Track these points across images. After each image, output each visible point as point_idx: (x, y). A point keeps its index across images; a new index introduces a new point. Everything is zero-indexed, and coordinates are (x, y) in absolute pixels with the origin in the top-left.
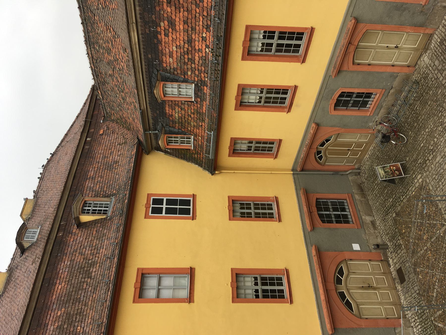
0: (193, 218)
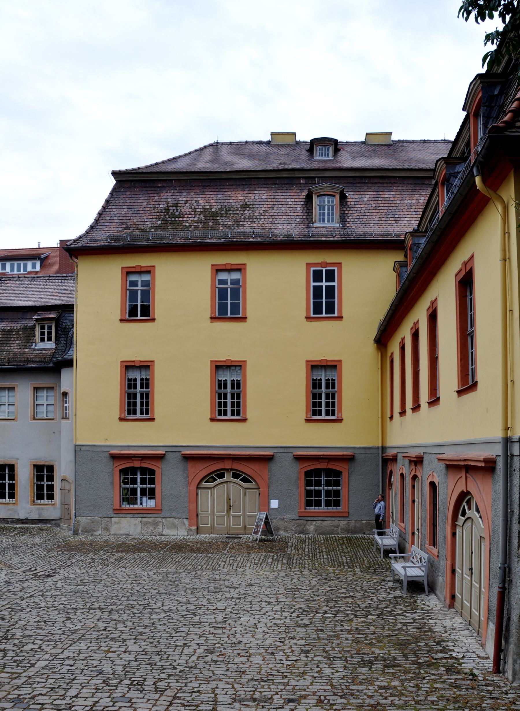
0: (308, 318)
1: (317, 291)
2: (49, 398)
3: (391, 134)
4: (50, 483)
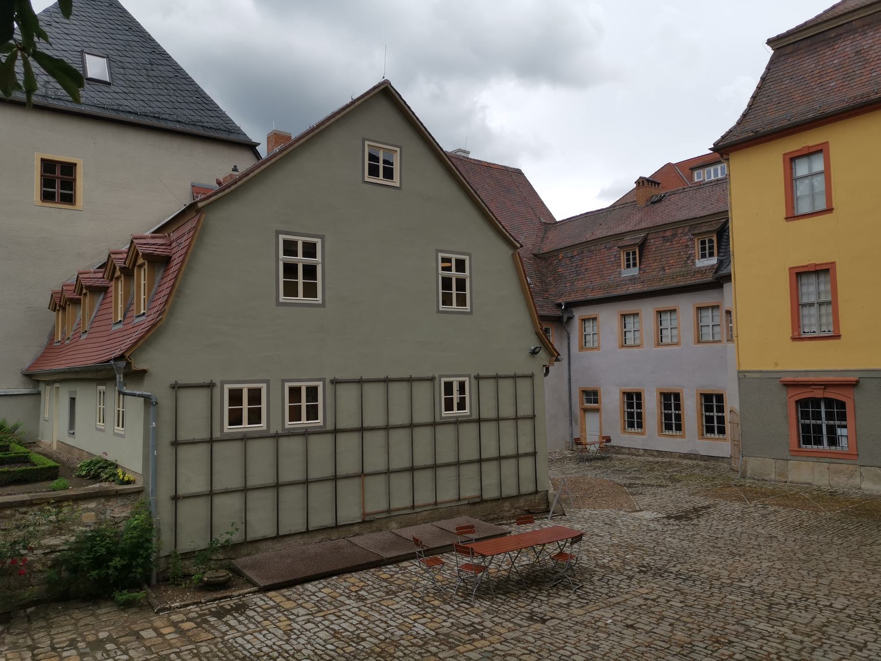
2: (715, 318)
4: (720, 414)
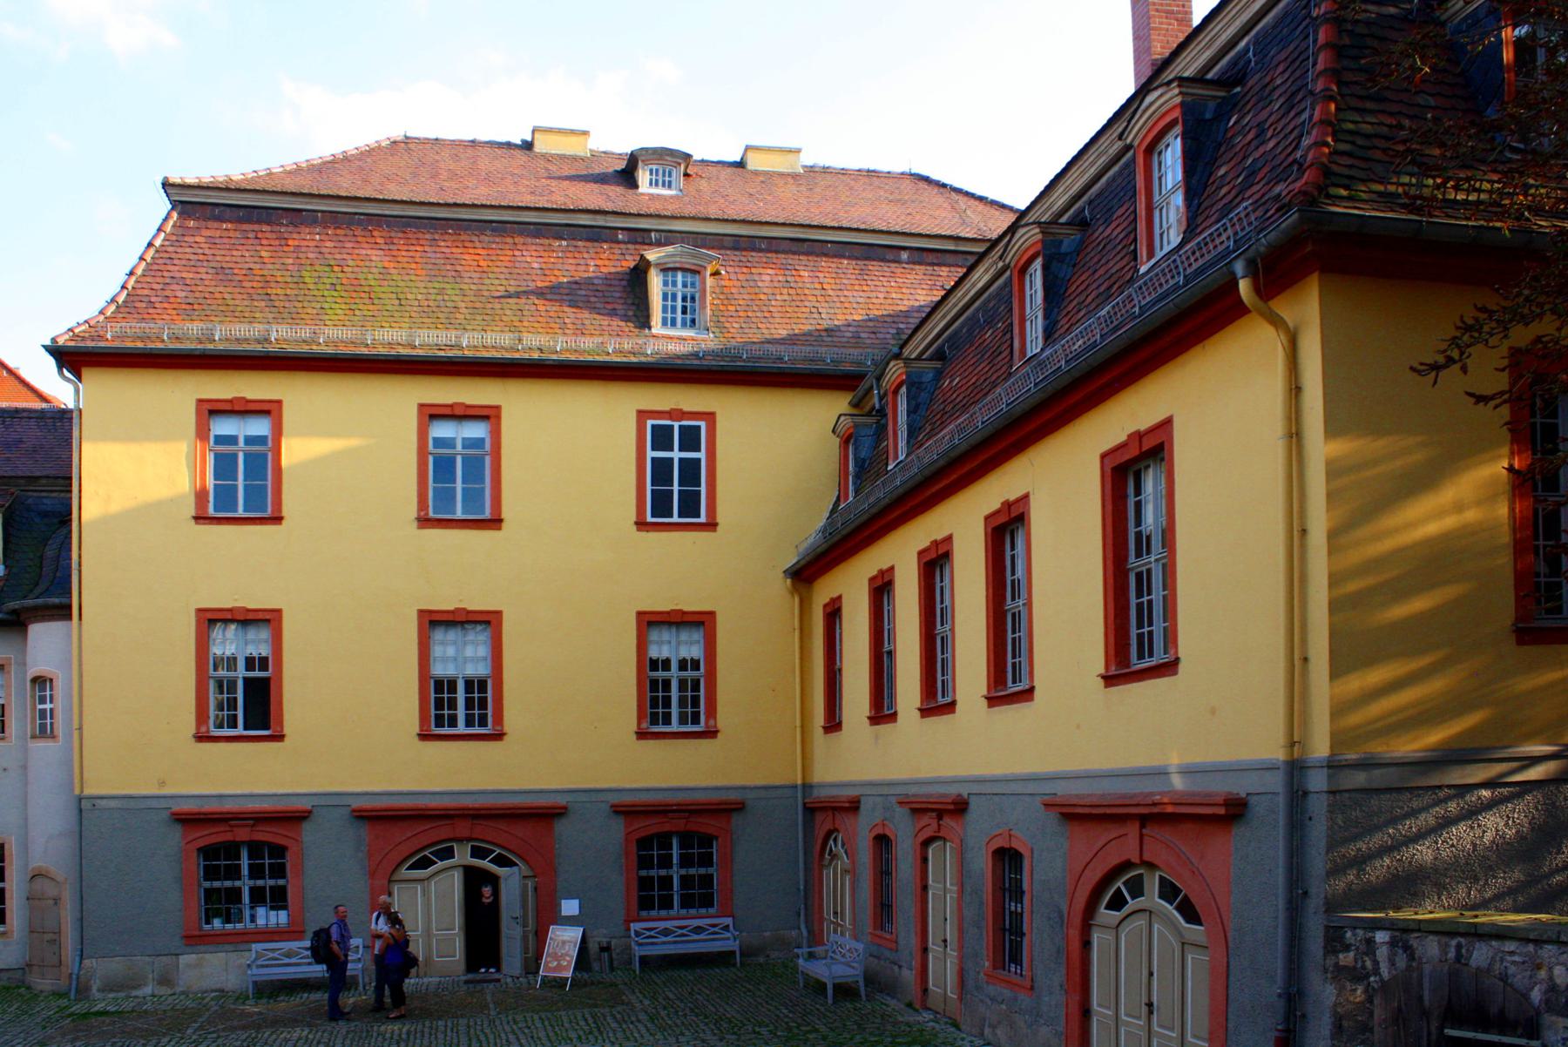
0: (641, 525)
1: (662, 470)
3: (798, 151)
